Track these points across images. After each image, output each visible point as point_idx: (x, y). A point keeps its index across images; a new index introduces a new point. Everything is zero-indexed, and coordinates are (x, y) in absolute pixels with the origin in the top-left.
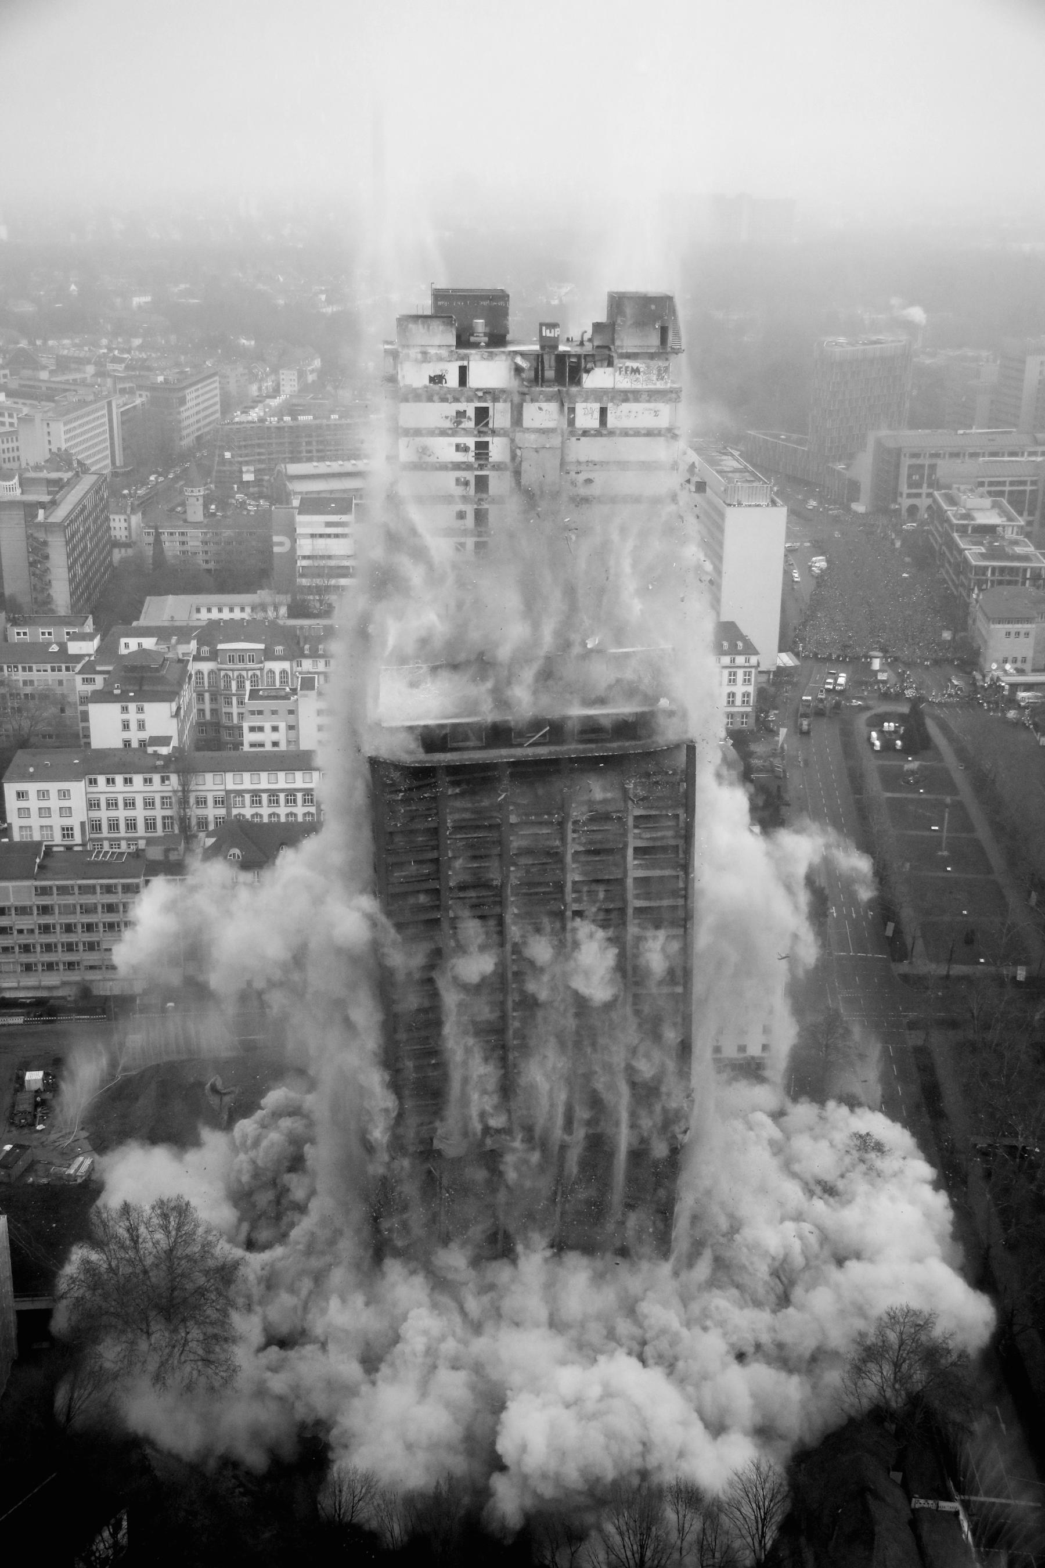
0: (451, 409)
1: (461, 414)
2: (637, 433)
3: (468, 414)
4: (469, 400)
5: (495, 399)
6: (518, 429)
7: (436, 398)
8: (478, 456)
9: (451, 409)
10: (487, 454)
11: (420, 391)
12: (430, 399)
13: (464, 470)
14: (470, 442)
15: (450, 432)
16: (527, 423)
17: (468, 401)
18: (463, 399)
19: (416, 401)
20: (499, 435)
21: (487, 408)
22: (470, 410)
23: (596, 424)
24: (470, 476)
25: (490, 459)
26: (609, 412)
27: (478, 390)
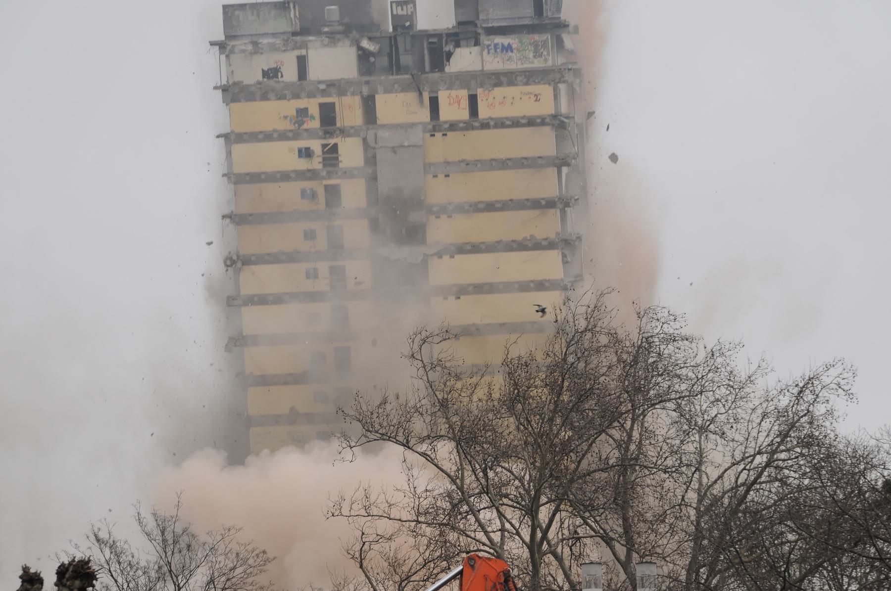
0: (290, 107)
1: (302, 113)
2: (516, 123)
3: (310, 112)
4: (311, 95)
5: (342, 93)
6: (371, 126)
9: (290, 107)
10: (337, 158)
12: (265, 97)
13: (310, 179)
14: (316, 145)
15: (291, 134)
19: (247, 100)
20: (349, 136)
21: (333, 104)
22: (313, 106)
23: (465, 115)
24: (318, 187)
25: (341, 165)
27: (320, 82)
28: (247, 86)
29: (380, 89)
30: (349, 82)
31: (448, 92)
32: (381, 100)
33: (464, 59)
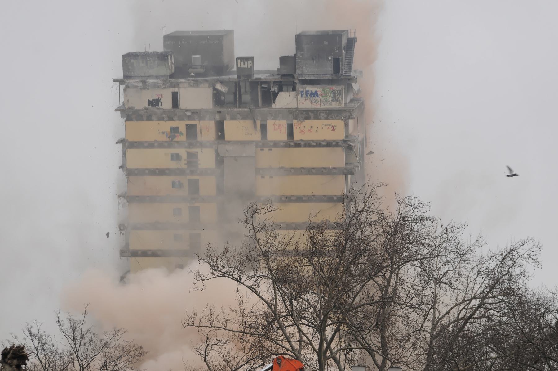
1: (175, 130)
3: (180, 130)
4: (181, 119)
5: (201, 119)
6: (221, 142)
7: (154, 117)
8: (189, 163)
9: (167, 126)
11: (142, 112)
12: (149, 118)
16: (227, 137)
17: (179, 120)
18: (175, 118)
19: (137, 120)
22: (182, 126)
26: (294, 127)
27: (187, 110)
28: (138, 110)
29: (228, 117)
30: (207, 111)
31: (274, 121)
32: (229, 125)
33: (285, 100)
